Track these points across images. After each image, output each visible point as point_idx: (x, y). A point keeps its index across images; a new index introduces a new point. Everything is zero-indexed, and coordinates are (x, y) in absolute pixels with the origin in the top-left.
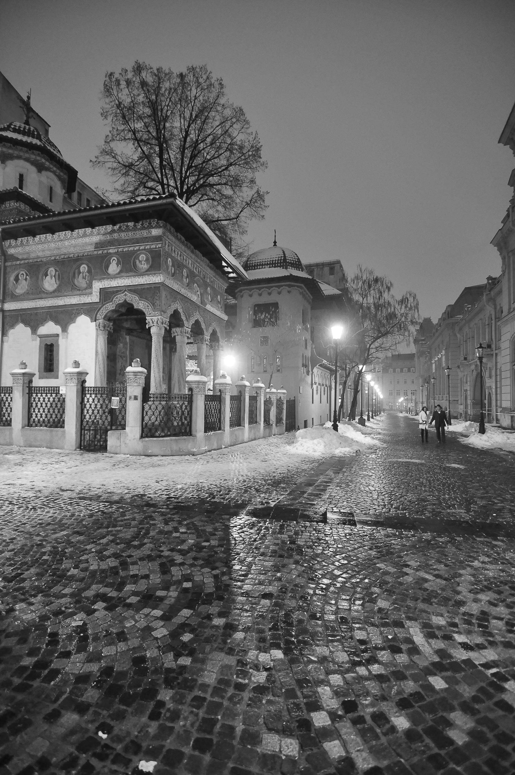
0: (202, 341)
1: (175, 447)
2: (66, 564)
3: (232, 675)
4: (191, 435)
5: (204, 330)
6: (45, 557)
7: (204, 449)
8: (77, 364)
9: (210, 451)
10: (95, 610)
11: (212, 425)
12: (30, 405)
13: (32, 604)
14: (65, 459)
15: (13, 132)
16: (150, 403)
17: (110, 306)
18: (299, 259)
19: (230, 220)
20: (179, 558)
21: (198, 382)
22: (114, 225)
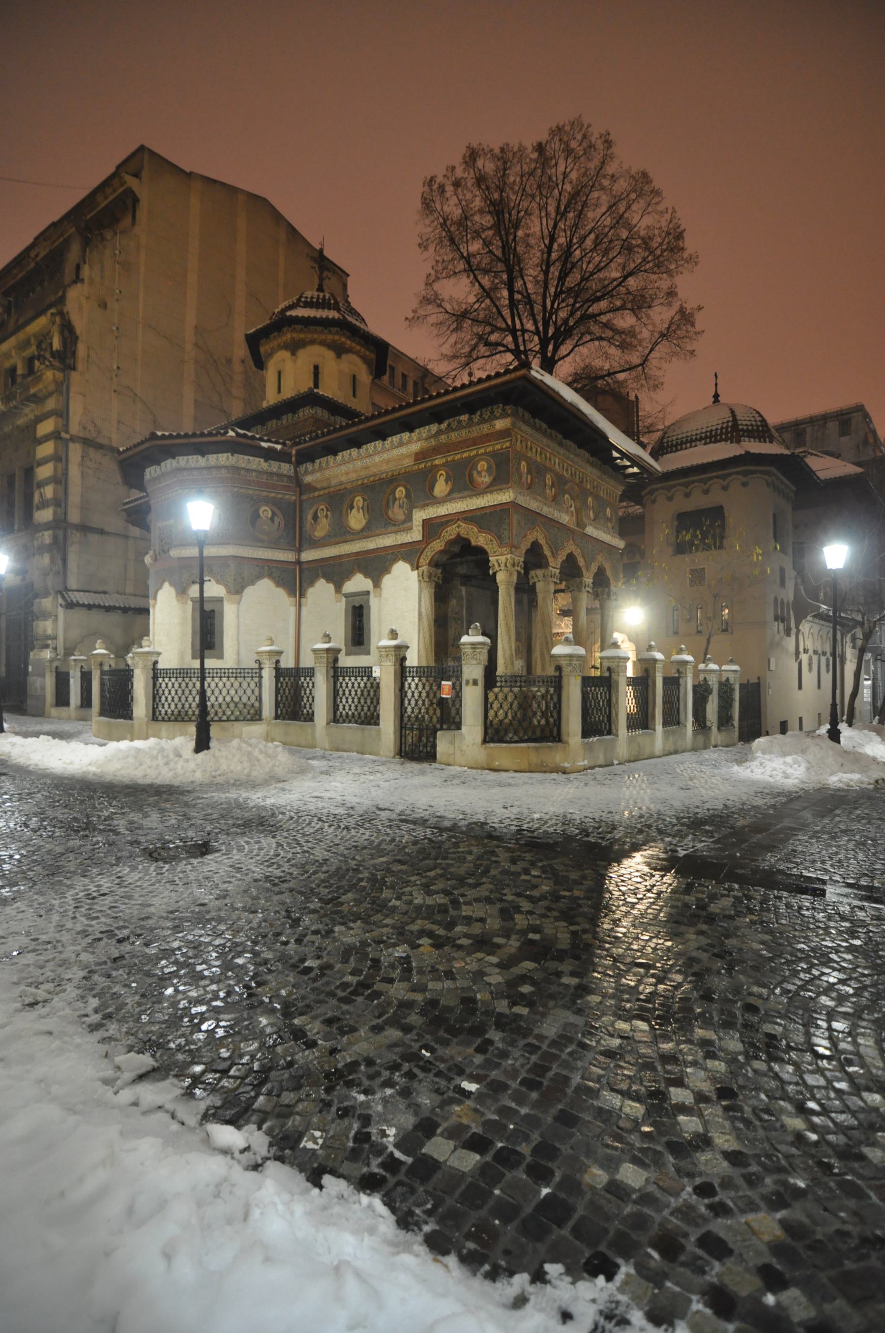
0: (580, 587)
1: (534, 758)
2: (386, 894)
3: (576, 1033)
4: (560, 740)
6: (363, 884)
7: (582, 763)
8: (394, 634)
9: (592, 768)
10: (420, 946)
13: (352, 929)
14: (381, 768)
15: (305, 307)
16: (496, 690)
17: (438, 545)
18: (764, 420)
20: (526, 906)
21: (570, 656)
22: (440, 422)
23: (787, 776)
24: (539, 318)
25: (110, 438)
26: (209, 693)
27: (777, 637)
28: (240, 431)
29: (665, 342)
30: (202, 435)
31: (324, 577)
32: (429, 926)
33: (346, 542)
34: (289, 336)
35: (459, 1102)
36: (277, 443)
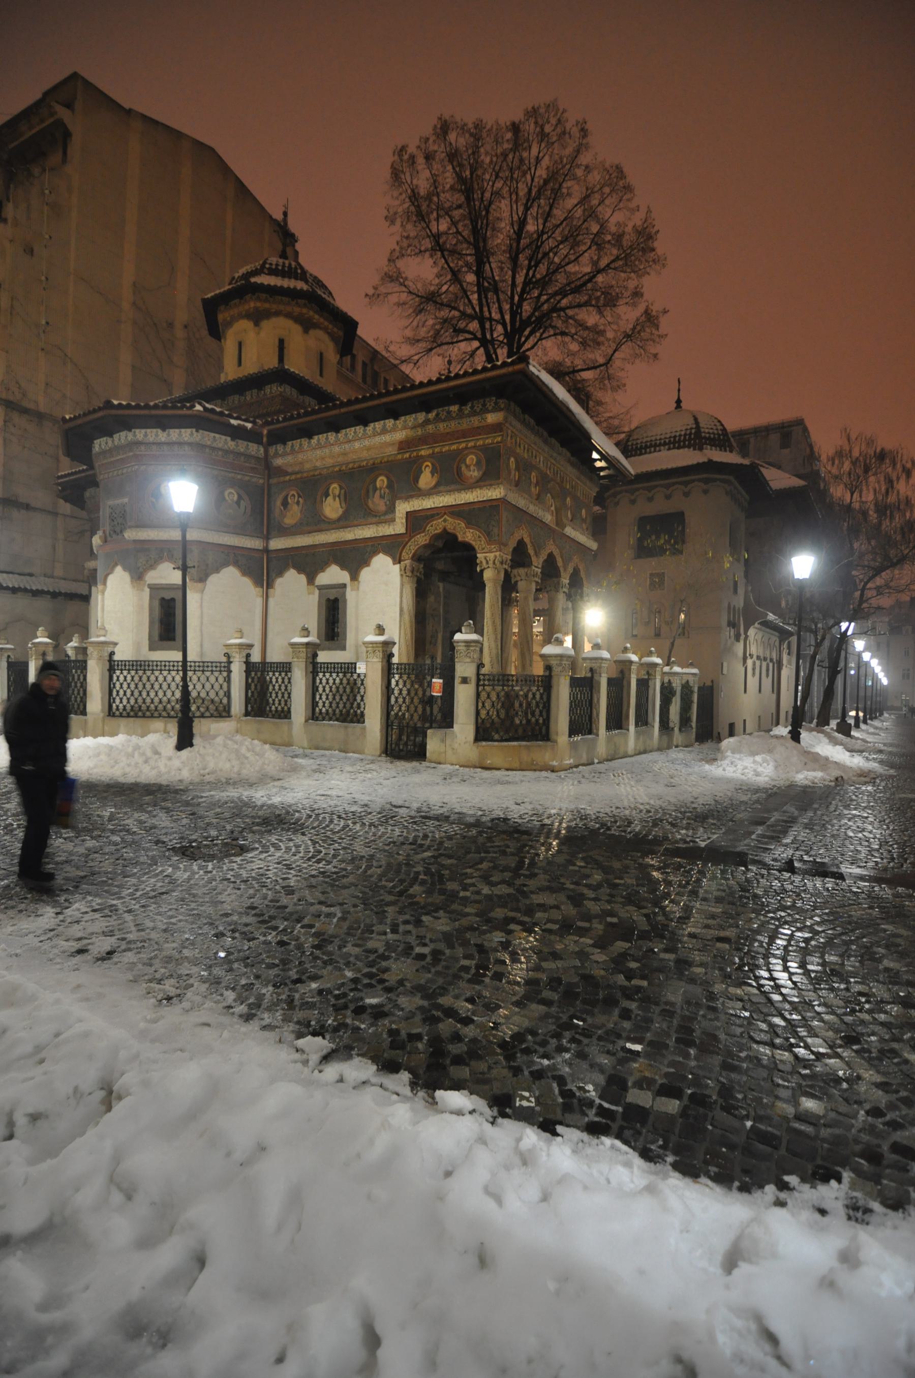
0: (557, 587)
5: (562, 570)
8: (380, 630)
9: (577, 766)
11: (582, 725)
12: (314, 689)
17: (422, 539)
18: (724, 429)
19: (595, 368)
22: (428, 412)
23: (757, 774)
24: (506, 307)
25: (36, 402)
26: (191, 688)
27: (729, 642)
28: (207, 405)
29: (629, 343)
30: (147, 407)
31: (294, 568)
32: (512, 914)
33: (320, 531)
34: (252, 305)
35: (635, 1061)
36: (246, 420)
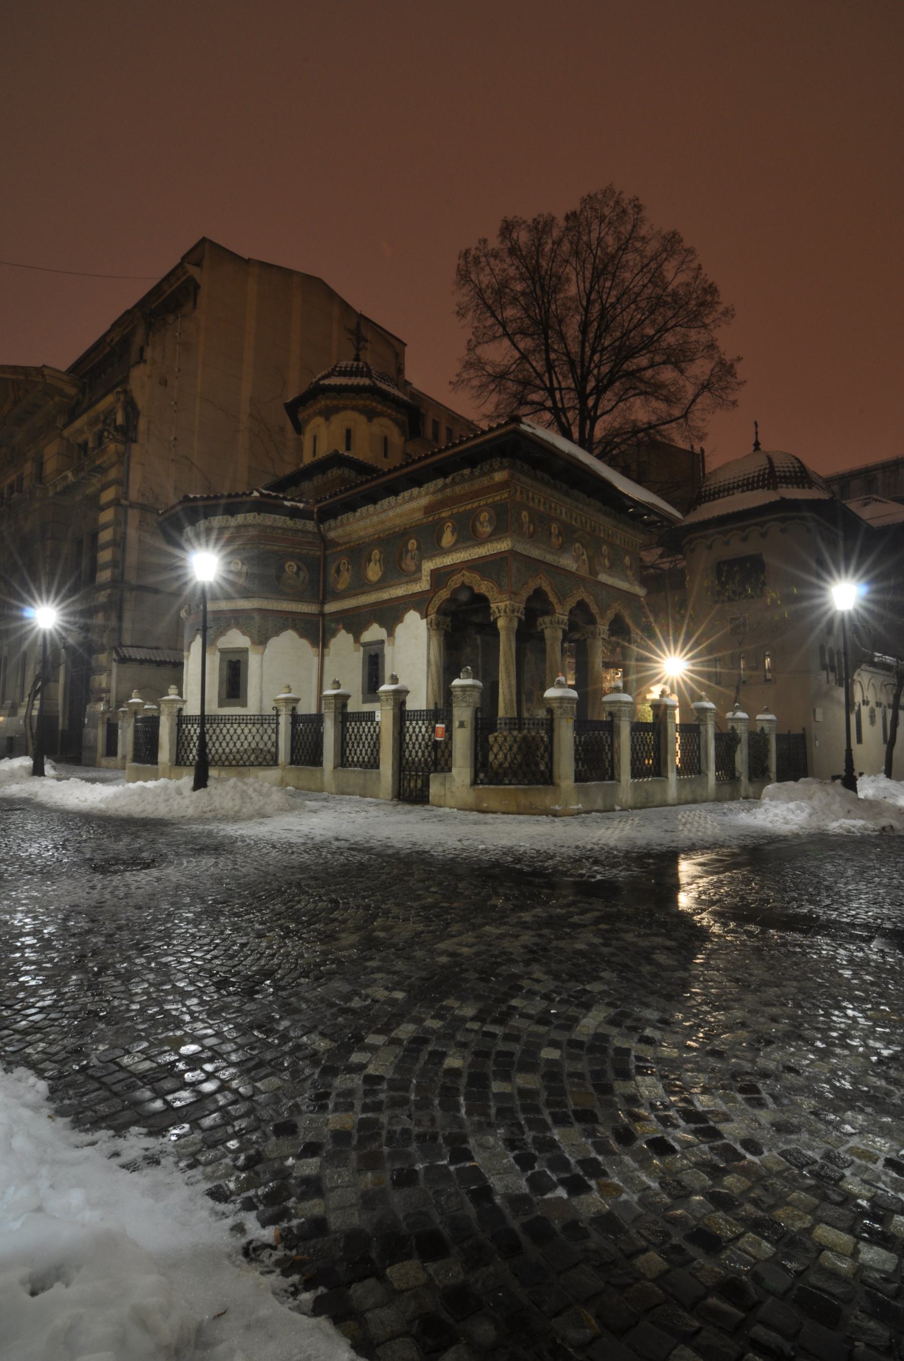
7: (575, 807)
9: (588, 812)
14: (367, 808)
15: (339, 376)
17: (444, 594)
18: (802, 466)
21: (561, 699)
22: (446, 477)
29: (706, 393)
33: (363, 593)
